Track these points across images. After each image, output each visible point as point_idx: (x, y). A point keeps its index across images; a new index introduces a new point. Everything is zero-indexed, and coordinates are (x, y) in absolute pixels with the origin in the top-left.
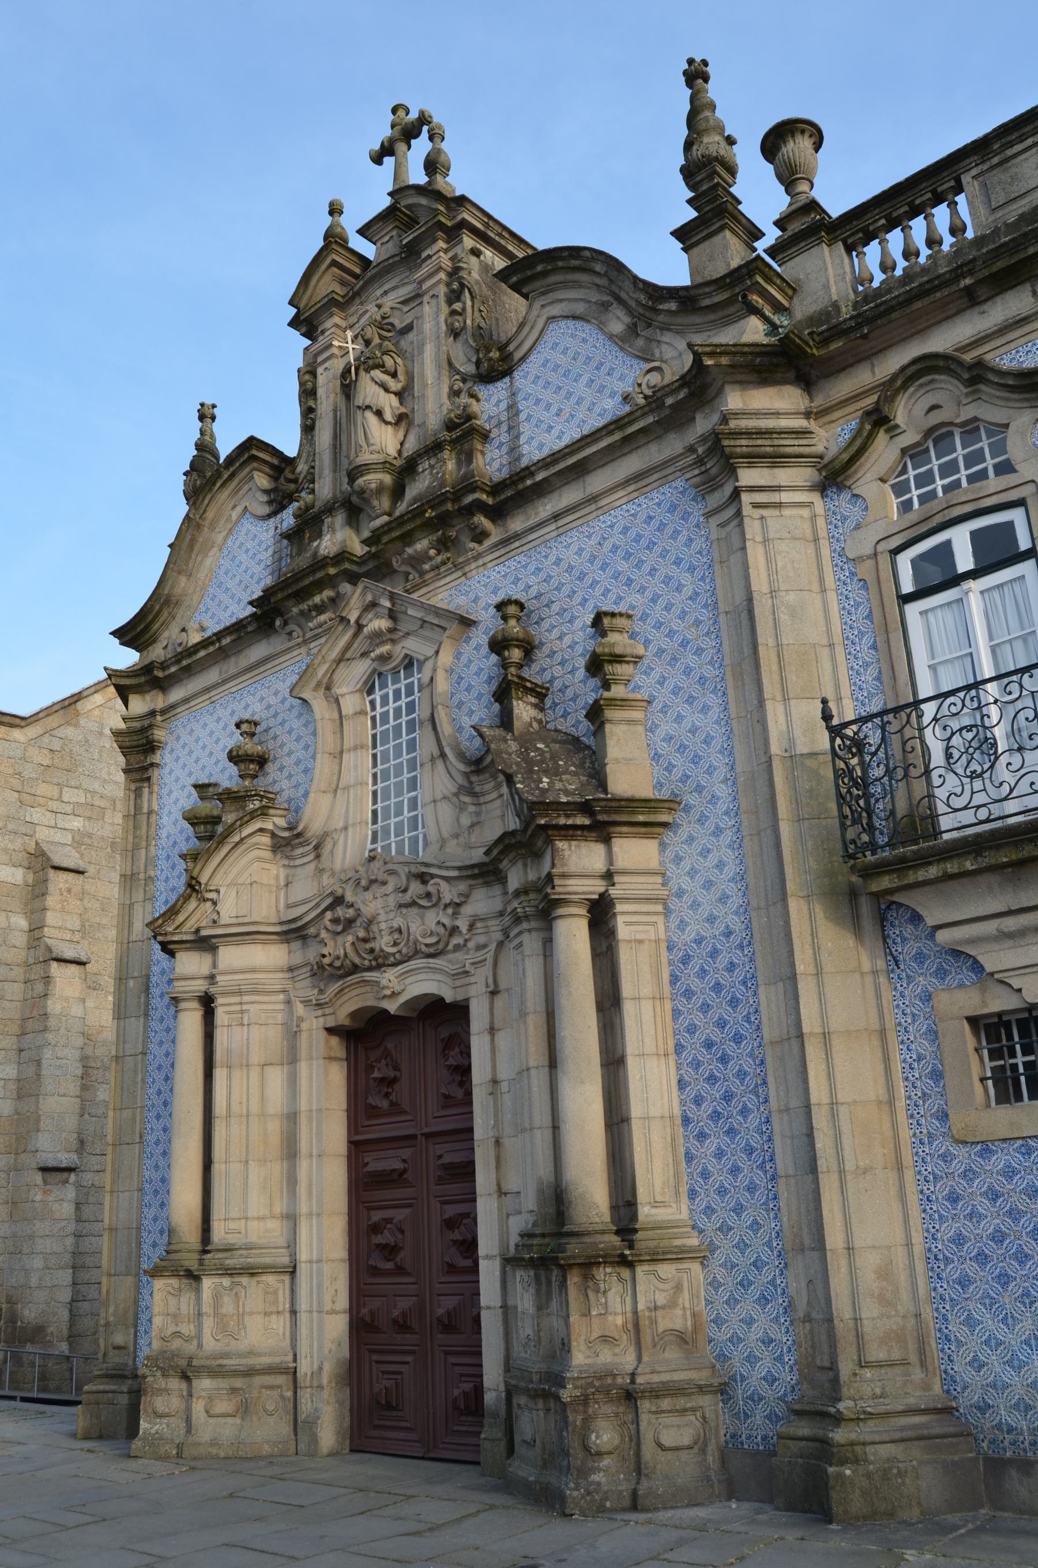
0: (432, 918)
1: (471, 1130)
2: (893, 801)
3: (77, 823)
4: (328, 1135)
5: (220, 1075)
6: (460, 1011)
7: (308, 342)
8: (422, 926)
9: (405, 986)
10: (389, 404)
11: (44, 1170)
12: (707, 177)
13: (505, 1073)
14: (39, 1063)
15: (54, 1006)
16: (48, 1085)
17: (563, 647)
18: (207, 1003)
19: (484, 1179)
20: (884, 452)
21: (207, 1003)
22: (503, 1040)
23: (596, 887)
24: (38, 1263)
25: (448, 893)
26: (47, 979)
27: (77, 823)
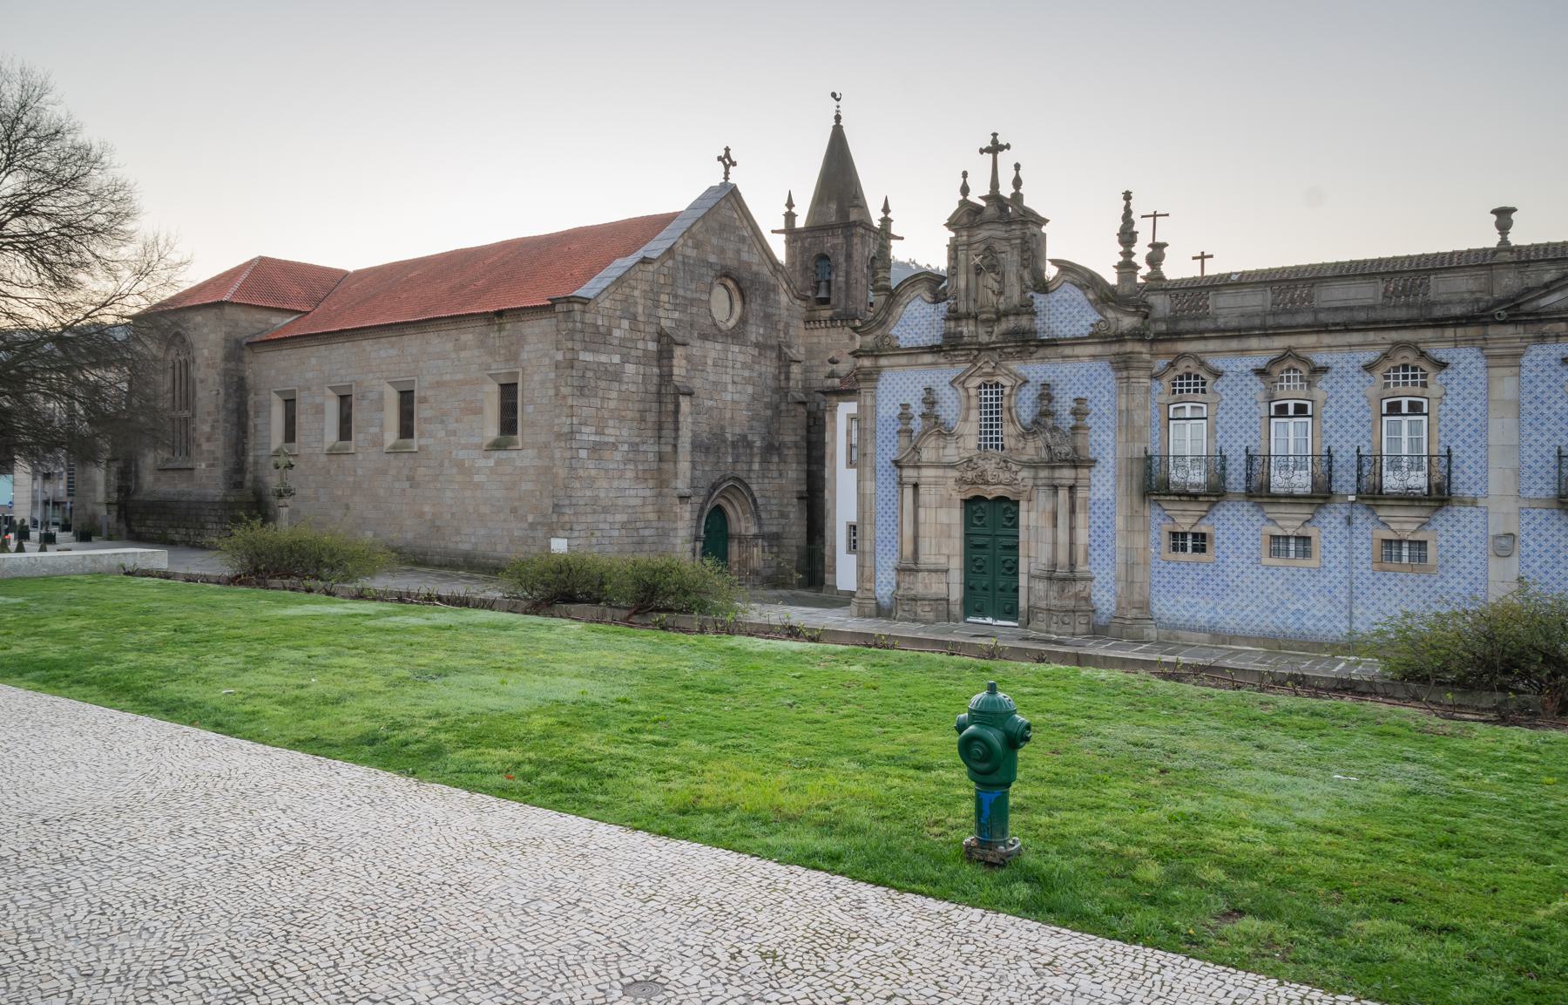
0: (1007, 475)
1: (1017, 537)
2: (1157, 475)
3: (676, 315)
4: (958, 532)
5: (922, 511)
6: (1017, 503)
7: (953, 234)
8: (1005, 476)
9: (992, 492)
10: (996, 286)
11: (681, 497)
12: (1127, 236)
13: (1032, 523)
14: (675, 446)
15: (681, 419)
16: (681, 457)
17: (1064, 404)
18: (916, 486)
19: (1022, 551)
20: (1173, 374)
21: (916, 486)
22: (1033, 515)
23: (1071, 482)
24: (679, 541)
25: (1014, 468)
26: (677, 405)
27: (676, 315)
